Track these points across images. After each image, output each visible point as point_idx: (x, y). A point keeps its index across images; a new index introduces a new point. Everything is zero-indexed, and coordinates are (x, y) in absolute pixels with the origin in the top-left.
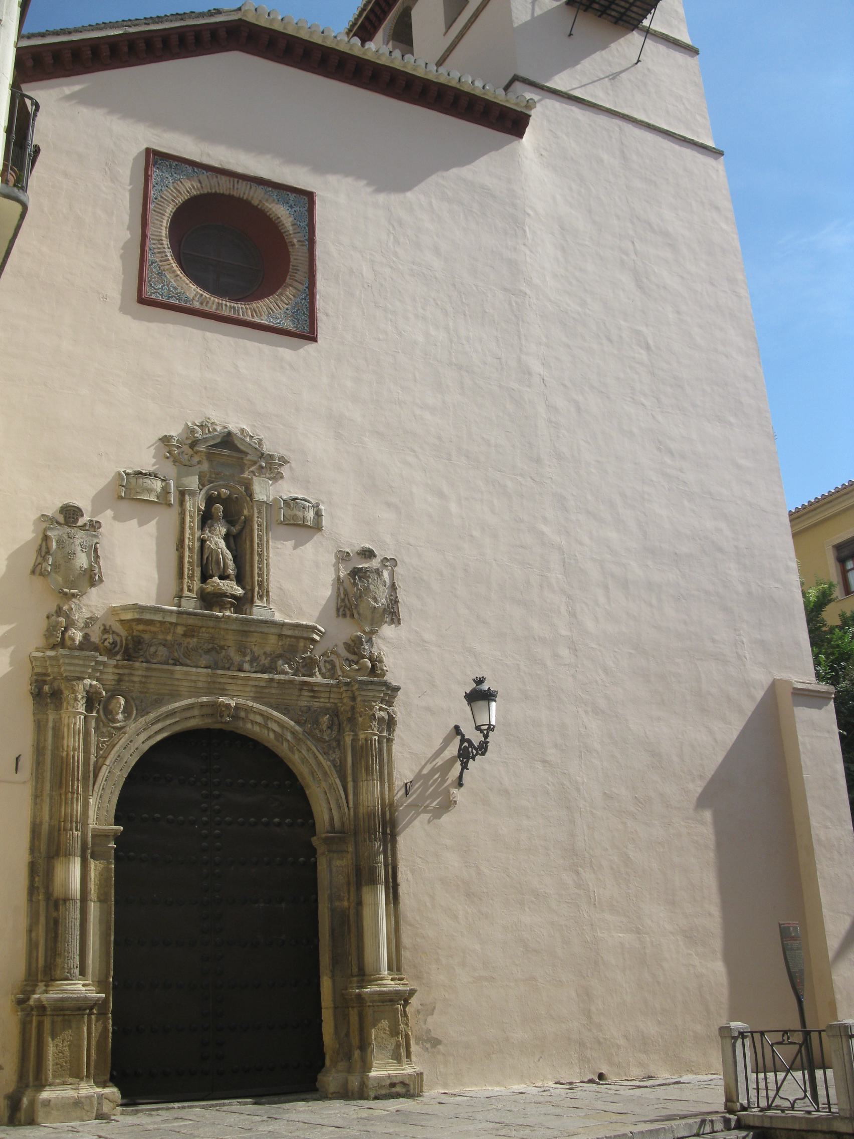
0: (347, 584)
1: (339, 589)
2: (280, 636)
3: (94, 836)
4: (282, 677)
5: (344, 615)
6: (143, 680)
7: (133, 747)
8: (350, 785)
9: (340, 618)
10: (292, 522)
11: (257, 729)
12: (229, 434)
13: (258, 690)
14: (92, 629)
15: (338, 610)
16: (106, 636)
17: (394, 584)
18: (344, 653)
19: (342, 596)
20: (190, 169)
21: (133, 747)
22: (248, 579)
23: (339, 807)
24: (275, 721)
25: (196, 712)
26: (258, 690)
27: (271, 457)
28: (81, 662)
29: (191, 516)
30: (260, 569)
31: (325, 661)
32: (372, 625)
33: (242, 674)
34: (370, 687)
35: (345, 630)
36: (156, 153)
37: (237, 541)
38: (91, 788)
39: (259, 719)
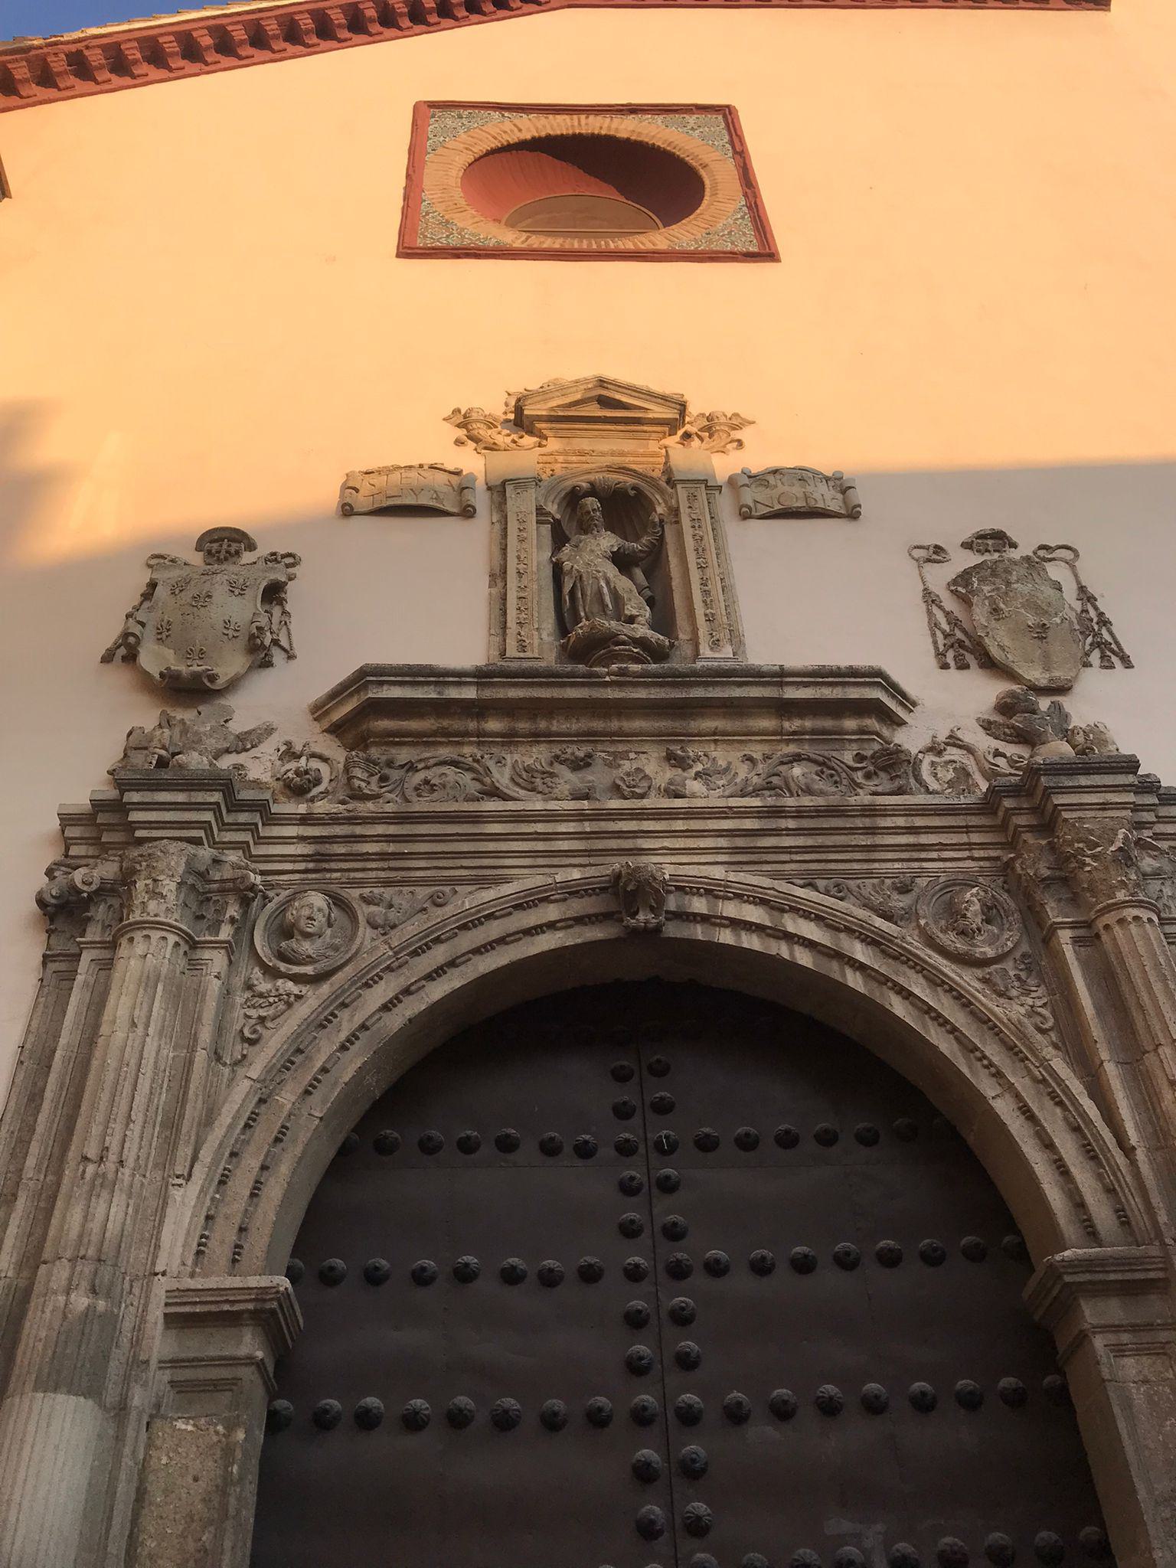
0: (950, 603)
1: (930, 613)
2: (786, 708)
3: (173, 1321)
4: (806, 801)
5: (963, 666)
6: (392, 848)
7: (347, 1022)
8: (1112, 1072)
9: (953, 671)
10: (777, 507)
11: (751, 942)
12: (602, 382)
13: (740, 842)
14: (254, 752)
15: (940, 655)
16: (293, 765)
17: (1082, 589)
18: (984, 743)
19: (946, 627)
20: (496, 115)
21: (347, 1022)
22: (681, 621)
23: (1091, 1153)
24: (806, 915)
25: (552, 912)
26: (740, 842)
27: (710, 418)
28: (181, 797)
29: (521, 522)
30: (706, 593)
31: (933, 763)
32: (1047, 668)
33: (678, 803)
34: (1083, 781)
35: (979, 693)
36: (433, 105)
37: (646, 562)
38: (184, 1152)
39: (754, 914)
